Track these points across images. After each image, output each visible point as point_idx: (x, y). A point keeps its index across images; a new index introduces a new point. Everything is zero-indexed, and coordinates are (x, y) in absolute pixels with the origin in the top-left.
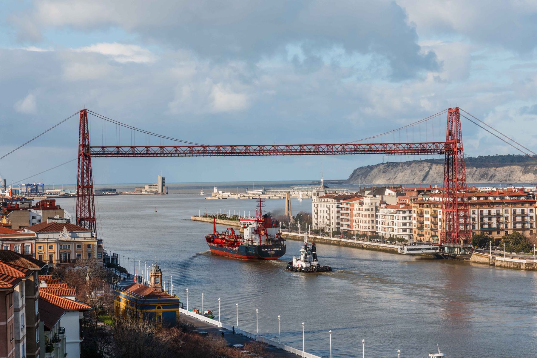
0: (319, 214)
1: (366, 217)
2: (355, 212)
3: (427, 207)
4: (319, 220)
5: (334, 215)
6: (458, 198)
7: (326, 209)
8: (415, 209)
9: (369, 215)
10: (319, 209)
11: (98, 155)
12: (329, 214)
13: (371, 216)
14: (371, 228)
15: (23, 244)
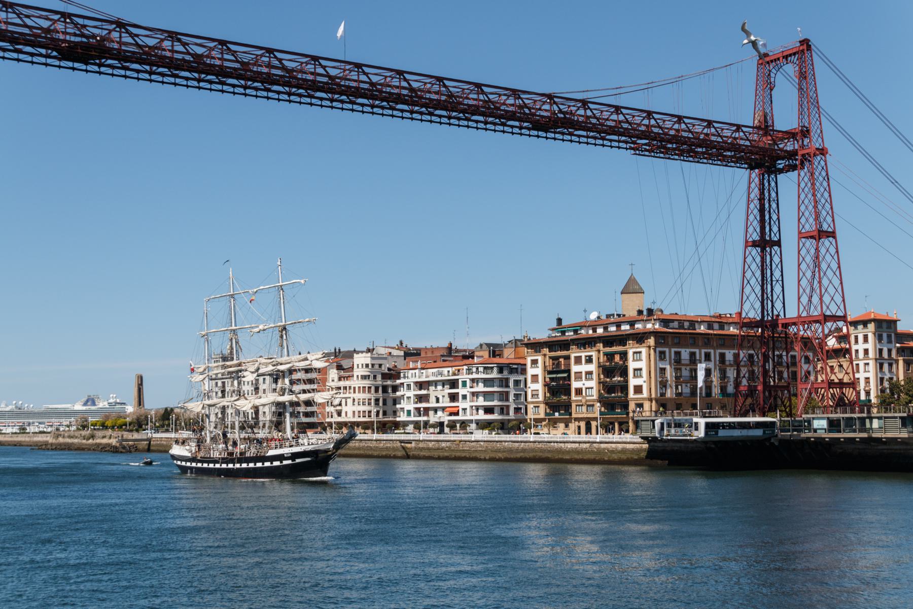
1: (364, 392)
8: (540, 359)
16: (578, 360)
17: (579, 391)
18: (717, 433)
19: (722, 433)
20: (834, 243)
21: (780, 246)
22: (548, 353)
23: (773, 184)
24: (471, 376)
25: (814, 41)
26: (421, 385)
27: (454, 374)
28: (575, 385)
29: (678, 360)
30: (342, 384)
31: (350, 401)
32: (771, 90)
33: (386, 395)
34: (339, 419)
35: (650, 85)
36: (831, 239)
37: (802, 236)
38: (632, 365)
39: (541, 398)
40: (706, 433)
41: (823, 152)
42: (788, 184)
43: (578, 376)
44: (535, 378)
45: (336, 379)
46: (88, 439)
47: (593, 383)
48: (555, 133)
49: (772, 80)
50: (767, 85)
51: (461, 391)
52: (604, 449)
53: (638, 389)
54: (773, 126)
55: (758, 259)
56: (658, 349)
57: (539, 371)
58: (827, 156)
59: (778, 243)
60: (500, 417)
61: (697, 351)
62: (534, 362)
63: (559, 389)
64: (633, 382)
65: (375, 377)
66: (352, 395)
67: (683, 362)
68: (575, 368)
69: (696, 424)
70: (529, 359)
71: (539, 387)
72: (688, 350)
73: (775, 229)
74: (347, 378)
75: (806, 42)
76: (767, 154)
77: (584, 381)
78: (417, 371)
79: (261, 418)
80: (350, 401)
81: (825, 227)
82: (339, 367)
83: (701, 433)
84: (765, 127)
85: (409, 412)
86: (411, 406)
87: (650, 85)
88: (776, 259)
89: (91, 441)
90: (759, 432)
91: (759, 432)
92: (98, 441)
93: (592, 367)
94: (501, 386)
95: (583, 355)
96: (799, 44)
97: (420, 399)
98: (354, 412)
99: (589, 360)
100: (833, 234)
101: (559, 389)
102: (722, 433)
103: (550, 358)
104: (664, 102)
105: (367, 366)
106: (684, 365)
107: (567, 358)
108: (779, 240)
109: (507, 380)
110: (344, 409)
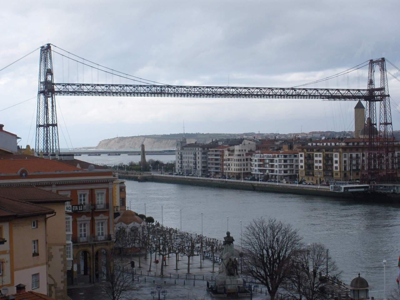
0: (184, 160)
1: (239, 161)
2: (225, 158)
3: (318, 151)
4: (184, 164)
5: (199, 160)
6: (350, 142)
7: (192, 156)
8: (303, 154)
9: (241, 160)
10: (184, 156)
11: (60, 92)
12: (195, 159)
13: (242, 160)
14: (242, 169)
15: (92, 191)
16: (316, 156)
17: (317, 167)
18: (348, 190)
19: (350, 190)
22: (306, 151)
24: (279, 159)
26: (260, 160)
27: (273, 157)
28: (316, 164)
29: (351, 156)
30: (230, 157)
31: (233, 165)
32: (374, 72)
33: (247, 162)
34: (229, 171)
35: (327, 79)
37: (380, 124)
38: (335, 159)
39: (303, 169)
40: (344, 191)
41: (389, 96)
43: (316, 161)
44: (301, 161)
45: (228, 155)
46: (125, 174)
47: (321, 165)
51: (275, 164)
52: (321, 191)
53: (336, 168)
56: (343, 154)
57: (303, 158)
60: (289, 174)
61: (359, 153)
62: (301, 156)
63: (309, 167)
64: (335, 165)
65: (243, 155)
66: (234, 162)
67: (353, 158)
68: (315, 159)
69: (341, 187)
70: (300, 154)
71: (303, 164)
72: (355, 153)
74: (232, 155)
77: (318, 164)
78: (259, 154)
79: (198, 169)
80: (233, 165)
82: (229, 150)
83: (342, 191)
85: (256, 170)
86: (257, 168)
87: (327, 79)
89: (126, 175)
90: (363, 190)
91: (363, 190)
92: (130, 175)
93: (321, 159)
94: (290, 162)
95: (318, 154)
96: (381, 59)
97: (260, 166)
98: (235, 169)
99: (320, 156)
101: (309, 167)
102: (350, 190)
103: (307, 154)
105: (240, 150)
106: (354, 159)
107: (313, 154)
109: (292, 160)
110: (231, 167)
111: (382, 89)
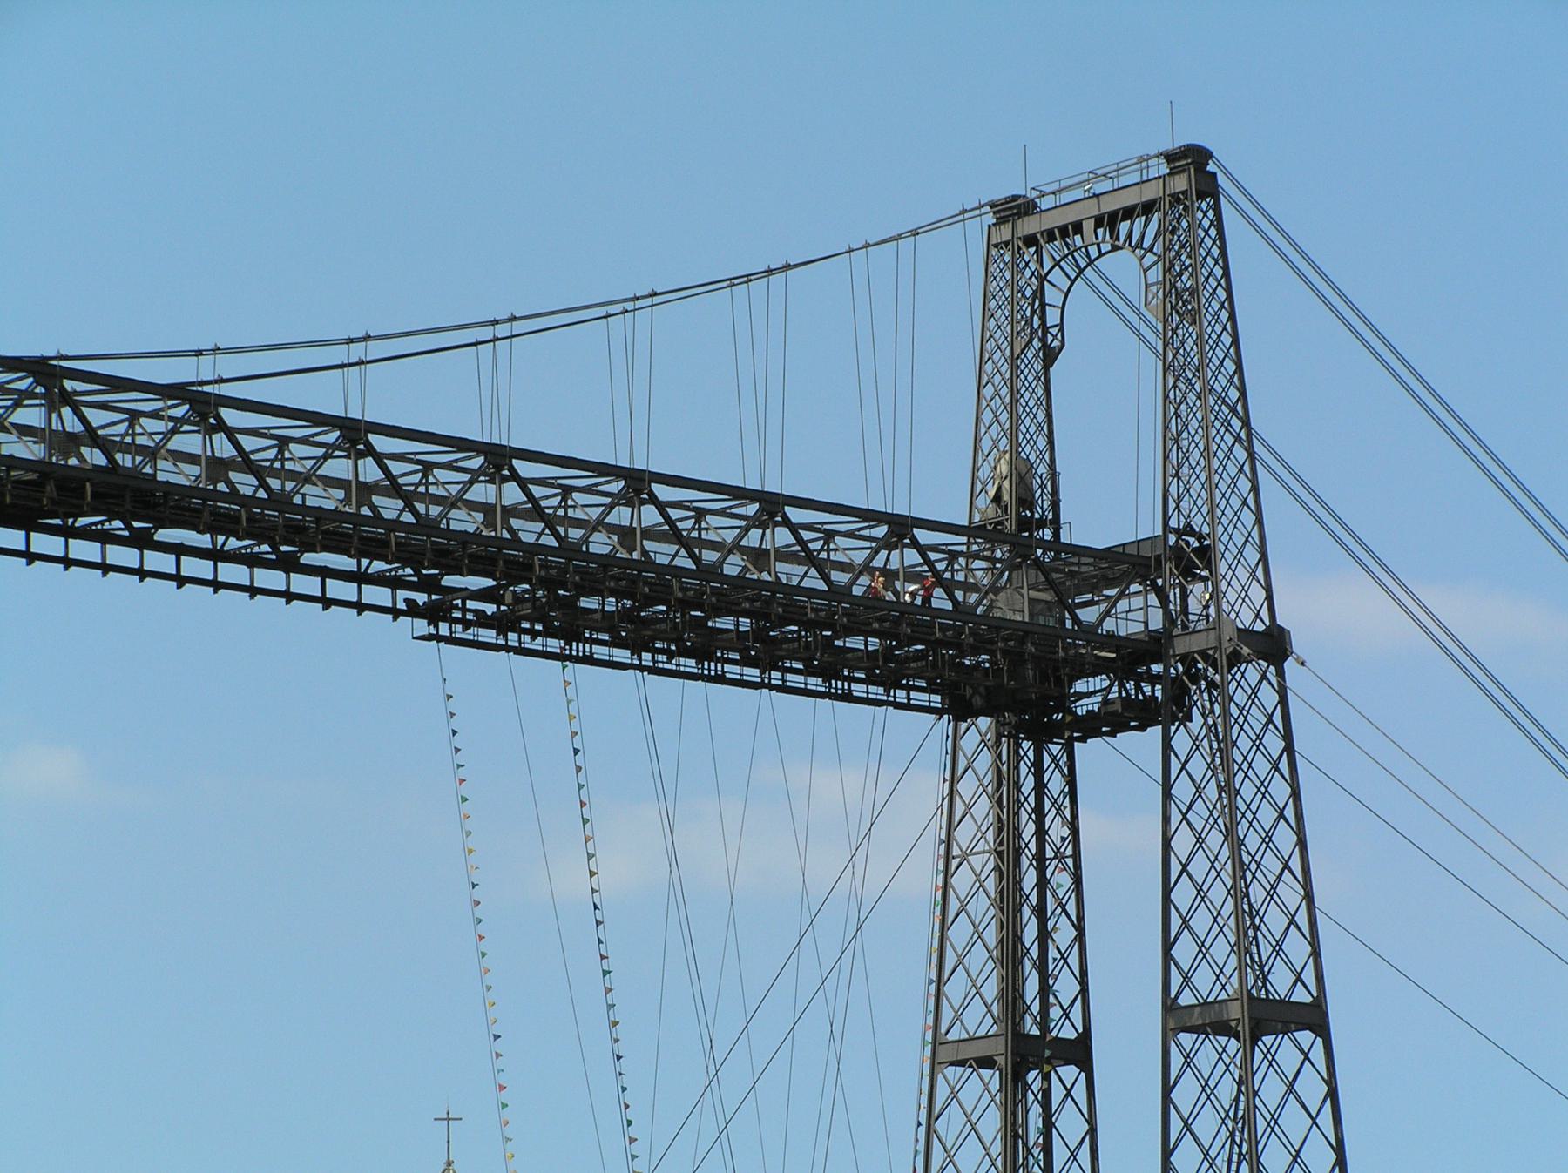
20: (1318, 1054)
21: (1086, 1065)
23: (1056, 784)
25: (1228, 159)
32: (1050, 356)
35: (502, 330)
36: (1305, 1037)
37: (1177, 1018)
41: (1273, 646)
42: (1117, 782)
48: (68, 533)
49: (1052, 317)
50: (1031, 341)
54: (1056, 524)
55: (991, 1124)
58: (1290, 665)
59: (1080, 1052)
73: (1065, 987)
75: (1192, 160)
76: (1031, 645)
81: (1280, 981)
84: (1020, 524)
88: (1070, 1124)
100: (1314, 1018)
104: (562, 407)
108: (1085, 1038)
111: (1180, 558)
